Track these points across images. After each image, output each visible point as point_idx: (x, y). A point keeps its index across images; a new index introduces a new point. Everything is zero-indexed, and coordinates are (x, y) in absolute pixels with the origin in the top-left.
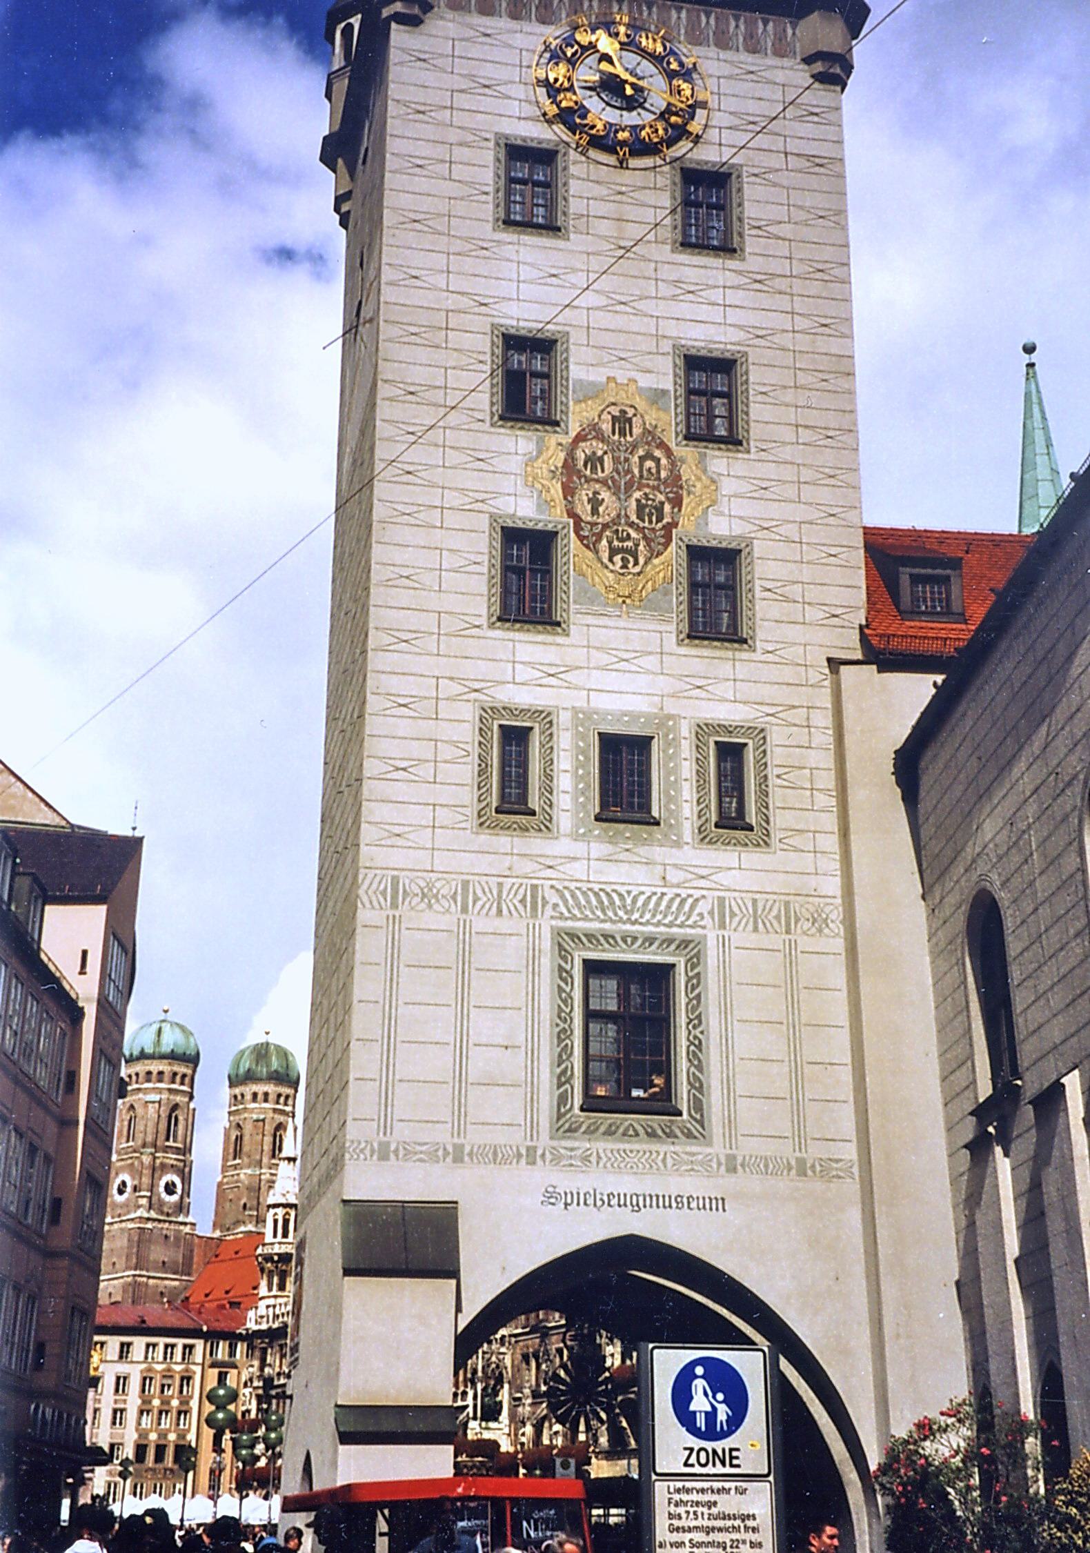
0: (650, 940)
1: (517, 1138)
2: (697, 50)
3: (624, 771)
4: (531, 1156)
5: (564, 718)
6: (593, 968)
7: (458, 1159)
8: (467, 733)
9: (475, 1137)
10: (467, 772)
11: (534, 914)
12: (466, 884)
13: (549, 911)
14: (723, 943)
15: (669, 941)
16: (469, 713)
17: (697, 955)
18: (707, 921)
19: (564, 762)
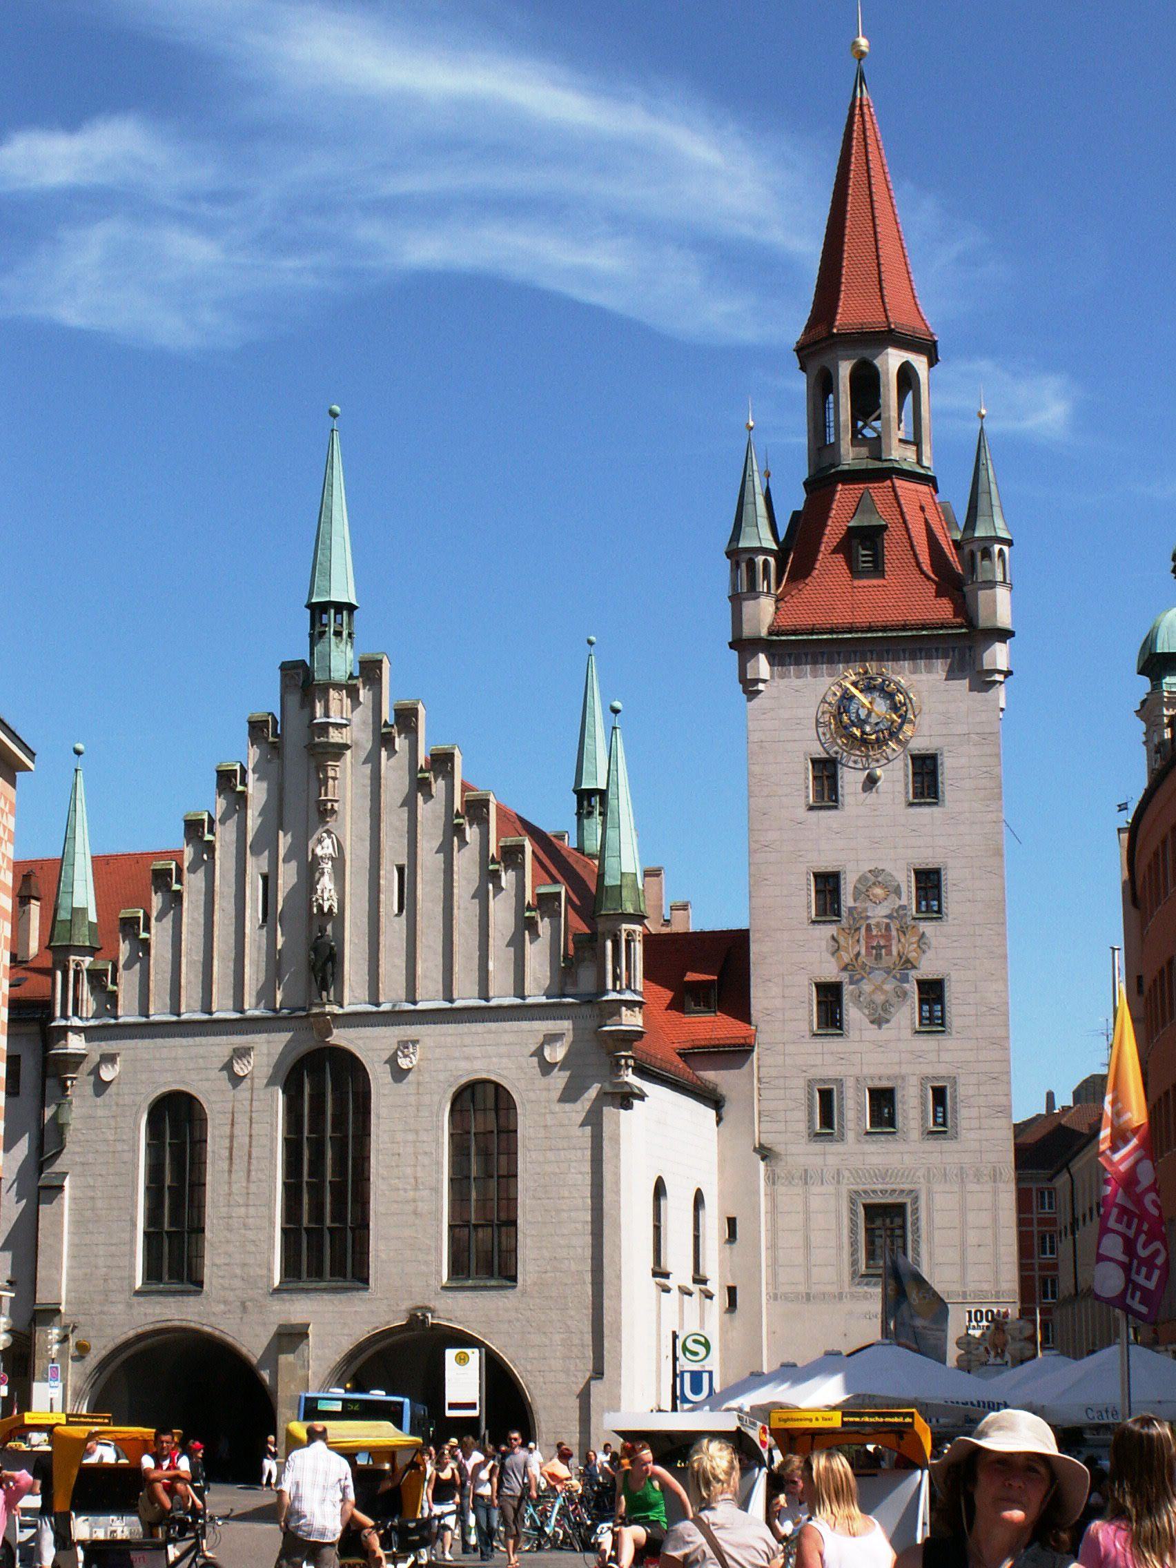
0: (894, 1191)
1: (833, 1289)
2: (914, 677)
3: (883, 1103)
4: (840, 1296)
5: (849, 1084)
6: (866, 1206)
7: (808, 1299)
8: (801, 1094)
9: (815, 1289)
10: (802, 1115)
11: (838, 1182)
12: (806, 1171)
13: (845, 1181)
14: (929, 1192)
15: (902, 1191)
16: (802, 1083)
17: (917, 1197)
18: (922, 1180)
19: (850, 1103)
